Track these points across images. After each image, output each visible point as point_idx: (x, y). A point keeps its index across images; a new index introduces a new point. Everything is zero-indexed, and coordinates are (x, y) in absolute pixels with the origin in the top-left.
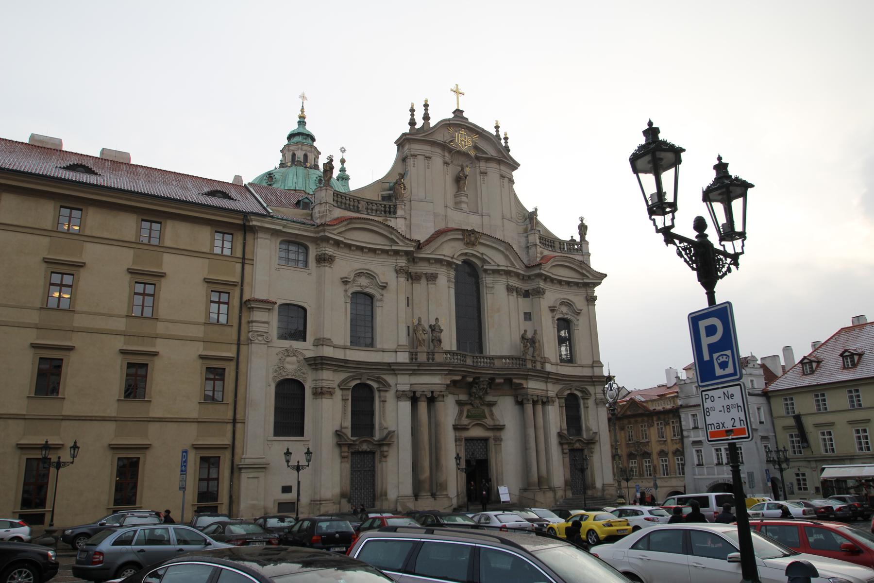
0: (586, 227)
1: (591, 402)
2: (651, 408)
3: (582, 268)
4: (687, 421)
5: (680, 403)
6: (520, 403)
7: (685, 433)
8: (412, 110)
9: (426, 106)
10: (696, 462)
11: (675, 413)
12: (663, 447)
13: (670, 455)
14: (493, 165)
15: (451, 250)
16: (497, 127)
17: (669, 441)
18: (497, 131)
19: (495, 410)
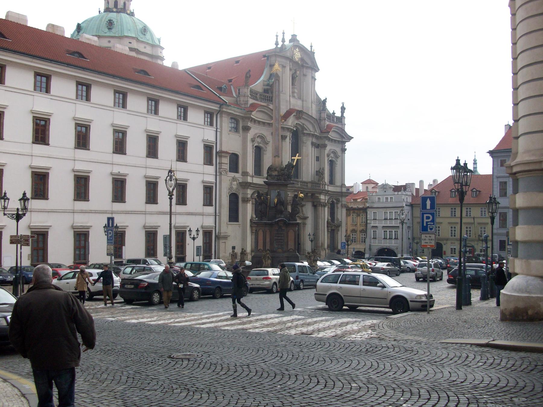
0: (345, 109)
1: (339, 205)
2: (350, 206)
3: (343, 133)
4: (370, 214)
5: (368, 205)
6: (315, 206)
7: (368, 222)
8: (277, 36)
9: (284, 33)
10: (372, 237)
11: (365, 210)
12: (354, 227)
13: (358, 232)
14: (310, 71)
15: (291, 122)
16: (311, 47)
17: (358, 224)
18: (311, 49)
19: (304, 209)
